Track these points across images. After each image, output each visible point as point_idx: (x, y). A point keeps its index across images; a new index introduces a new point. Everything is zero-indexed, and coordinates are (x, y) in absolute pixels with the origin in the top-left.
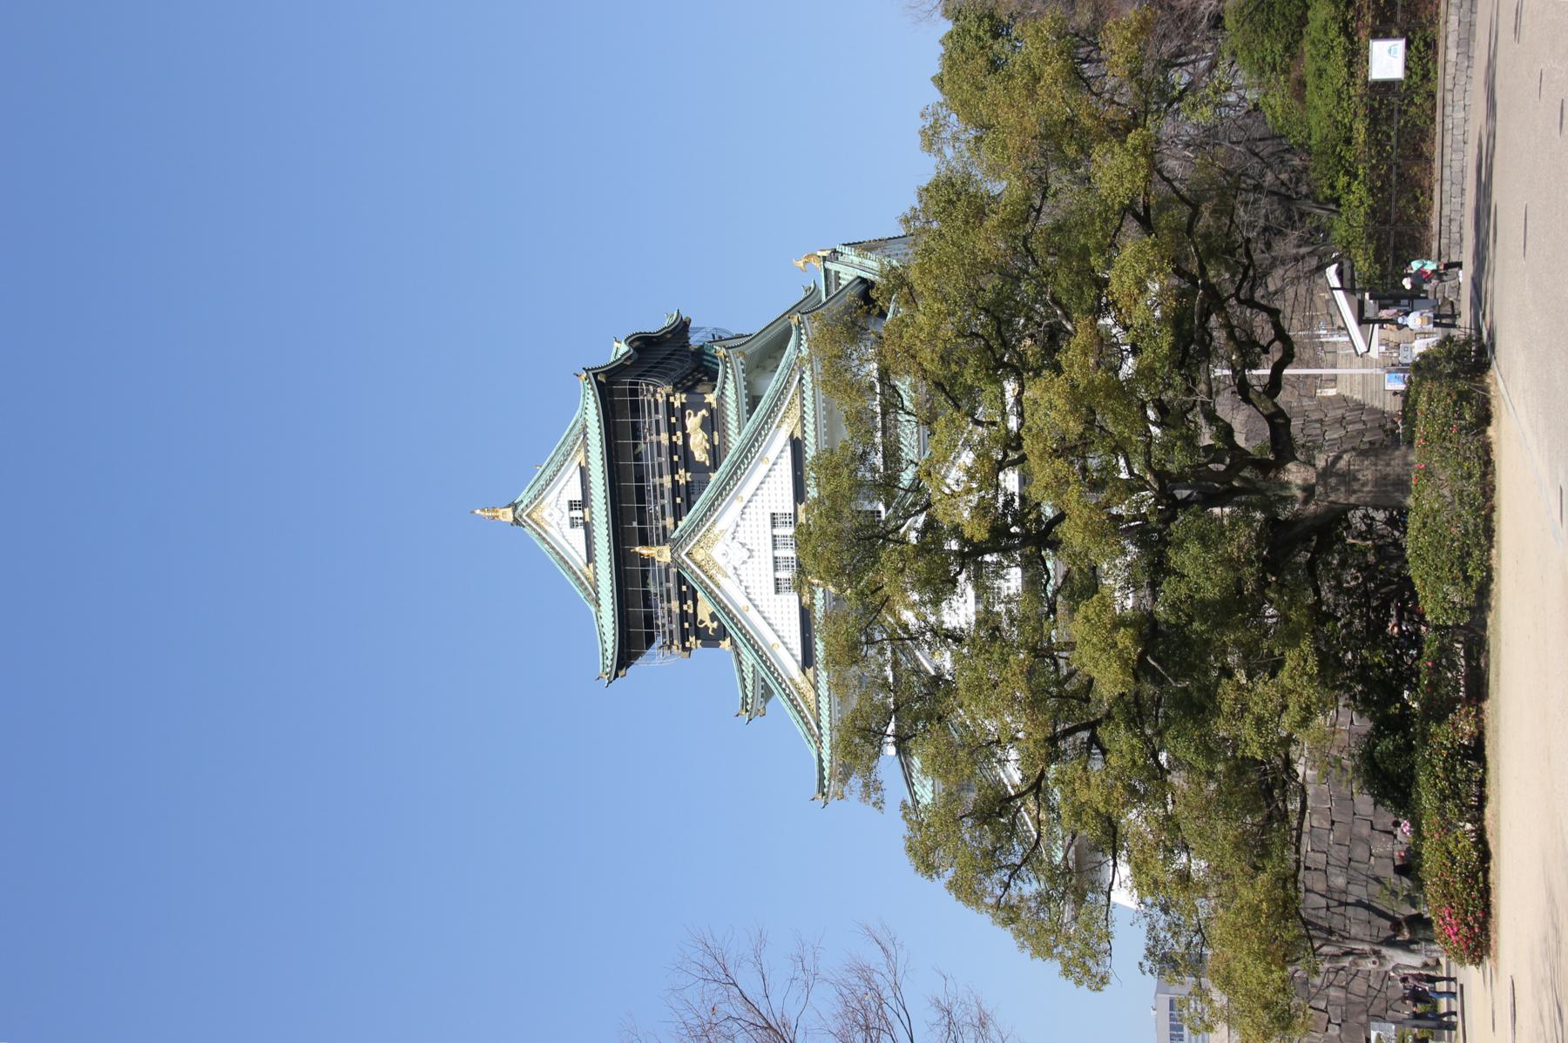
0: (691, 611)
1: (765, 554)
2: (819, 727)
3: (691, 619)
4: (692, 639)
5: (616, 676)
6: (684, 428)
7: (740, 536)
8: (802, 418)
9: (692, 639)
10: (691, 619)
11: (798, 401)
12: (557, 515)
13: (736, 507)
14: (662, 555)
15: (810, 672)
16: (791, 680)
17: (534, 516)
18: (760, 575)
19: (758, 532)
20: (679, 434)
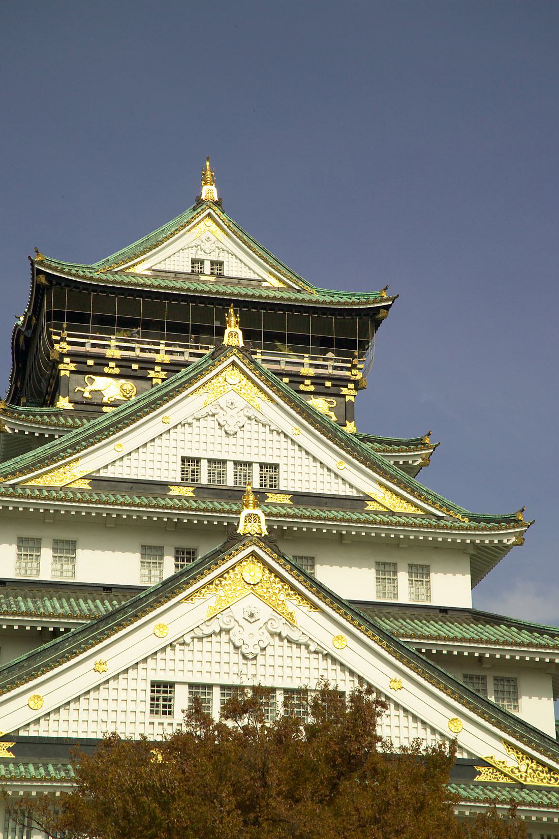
0: (106, 370)
1: (230, 451)
2: (13, 486)
3: (98, 369)
4: (72, 367)
5: (39, 272)
6: (315, 393)
7: (254, 426)
8: (393, 513)
9: (72, 367)
10: (98, 369)
11: (411, 510)
12: (207, 246)
13: (289, 426)
14: (233, 335)
15: (85, 485)
16: (77, 460)
17: (209, 222)
18: (206, 443)
19: (257, 447)
20: (312, 388)
